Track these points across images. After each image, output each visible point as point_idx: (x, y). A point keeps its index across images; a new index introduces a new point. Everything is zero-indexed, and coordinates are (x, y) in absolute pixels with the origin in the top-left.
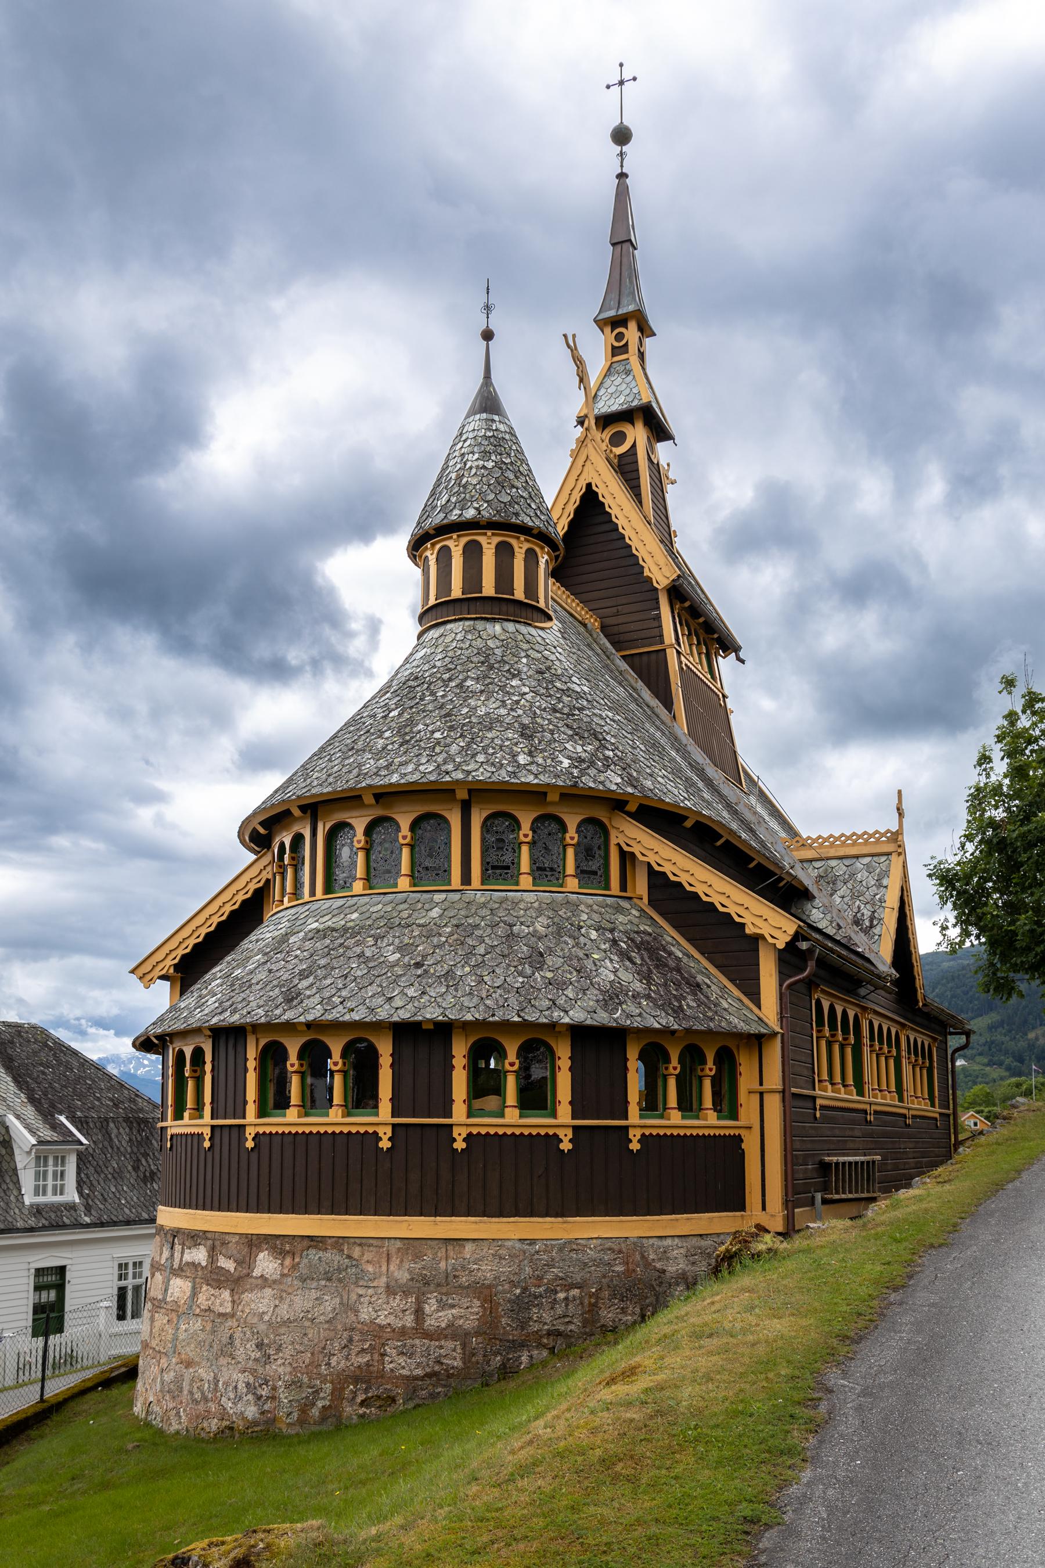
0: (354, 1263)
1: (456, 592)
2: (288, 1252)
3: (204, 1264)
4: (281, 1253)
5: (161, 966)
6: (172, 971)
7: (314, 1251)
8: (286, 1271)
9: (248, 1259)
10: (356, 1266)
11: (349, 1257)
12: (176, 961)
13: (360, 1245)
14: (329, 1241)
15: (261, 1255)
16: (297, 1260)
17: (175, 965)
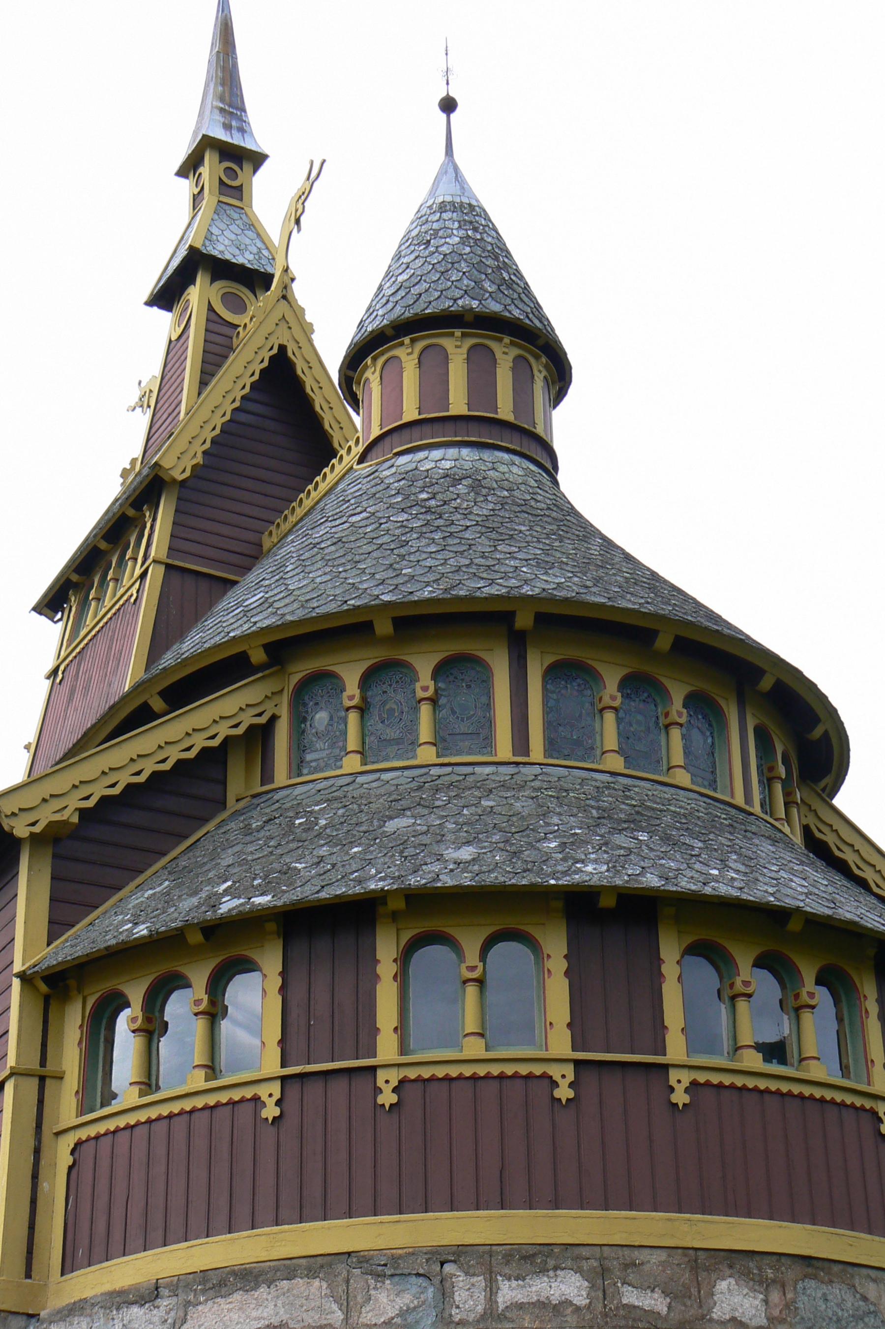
0: (872, 1308)
1: (410, 413)
2: (774, 1281)
3: (581, 1301)
4: (761, 1283)
5: (57, 804)
6: (75, 819)
7: (813, 1283)
8: (776, 1313)
9: (694, 1291)
10: (875, 1313)
11: (865, 1299)
12: (90, 803)
13: (874, 1281)
14: (836, 1268)
15: (722, 1285)
16: (790, 1296)
17: (82, 812)
